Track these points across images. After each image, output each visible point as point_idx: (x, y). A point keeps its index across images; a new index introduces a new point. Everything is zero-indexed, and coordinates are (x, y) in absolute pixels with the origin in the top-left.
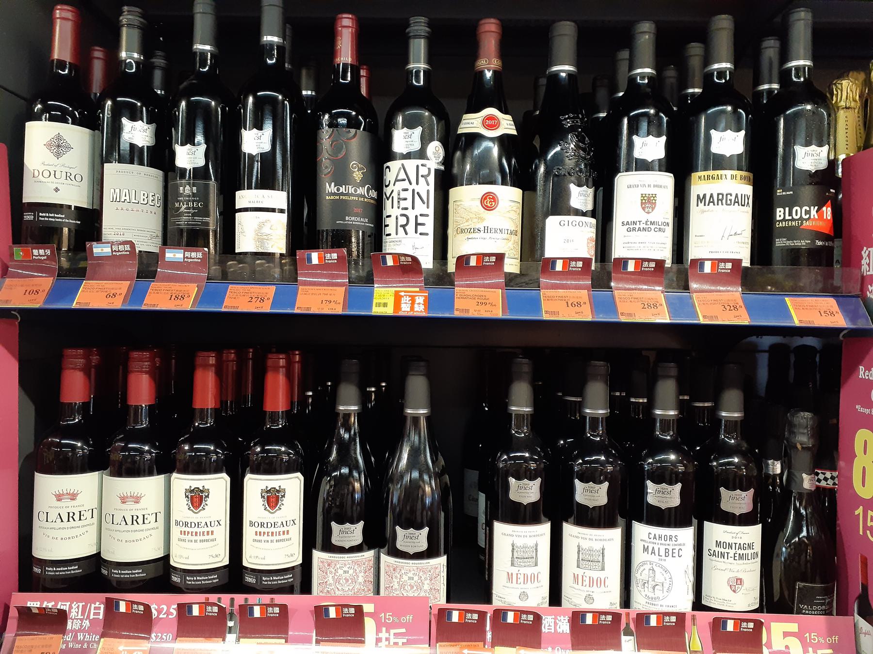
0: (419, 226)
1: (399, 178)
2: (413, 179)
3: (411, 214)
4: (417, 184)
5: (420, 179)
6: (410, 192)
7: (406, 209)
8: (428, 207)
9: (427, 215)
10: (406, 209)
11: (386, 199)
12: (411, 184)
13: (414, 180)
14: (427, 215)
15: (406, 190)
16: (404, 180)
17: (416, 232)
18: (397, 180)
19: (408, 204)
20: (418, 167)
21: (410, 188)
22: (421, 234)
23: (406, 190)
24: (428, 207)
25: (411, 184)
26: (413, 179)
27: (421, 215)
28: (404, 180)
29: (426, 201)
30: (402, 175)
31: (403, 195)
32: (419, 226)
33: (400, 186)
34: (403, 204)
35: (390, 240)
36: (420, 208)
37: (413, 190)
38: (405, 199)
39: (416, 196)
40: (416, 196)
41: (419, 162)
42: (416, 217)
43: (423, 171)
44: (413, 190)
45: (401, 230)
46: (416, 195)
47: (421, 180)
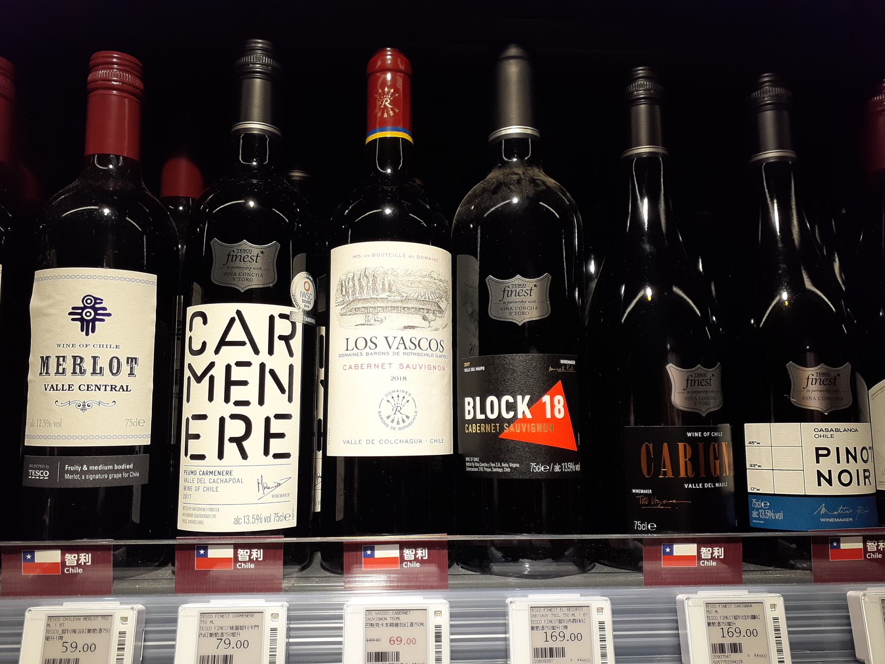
0: (271, 440)
1: (228, 339)
2: (262, 343)
3: (258, 416)
4: (271, 351)
5: (277, 341)
6: (255, 370)
7: (246, 403)
8: (290, 399)
9: (287, 417)
10: (246, 403)
11: (192, 378)
12: (256, 351)
13: (263, 345)
14: (287, 417)
15: (248, 364)
16: (242, 344)
17: (266, 452)
18: (223, 342)
19: (250, 393)
20: (272, 318)
21: (256, 361)
22: (276, 456)
23: (248, 364)
24: (290, 399)
25: (256, 351)
26: (262, 343)
27: (278, 417)
28: (242, 344)
29: (286, 387)
30: (237, 334)
31: (237, 374)
32: (271, 440)
33: (230, 355)
34: (237, 393)
35: (205, 469)
36: (276, 401)
37: (262, 366)
38: (244, 383)
39: (268, 378)
40: (268, 378)
41: (276, 310)
42: (268, 420)
43: (282, 328)
44: (262, 366)
45: (231, 449)
46: (268, 377)
47: (279, 345)
